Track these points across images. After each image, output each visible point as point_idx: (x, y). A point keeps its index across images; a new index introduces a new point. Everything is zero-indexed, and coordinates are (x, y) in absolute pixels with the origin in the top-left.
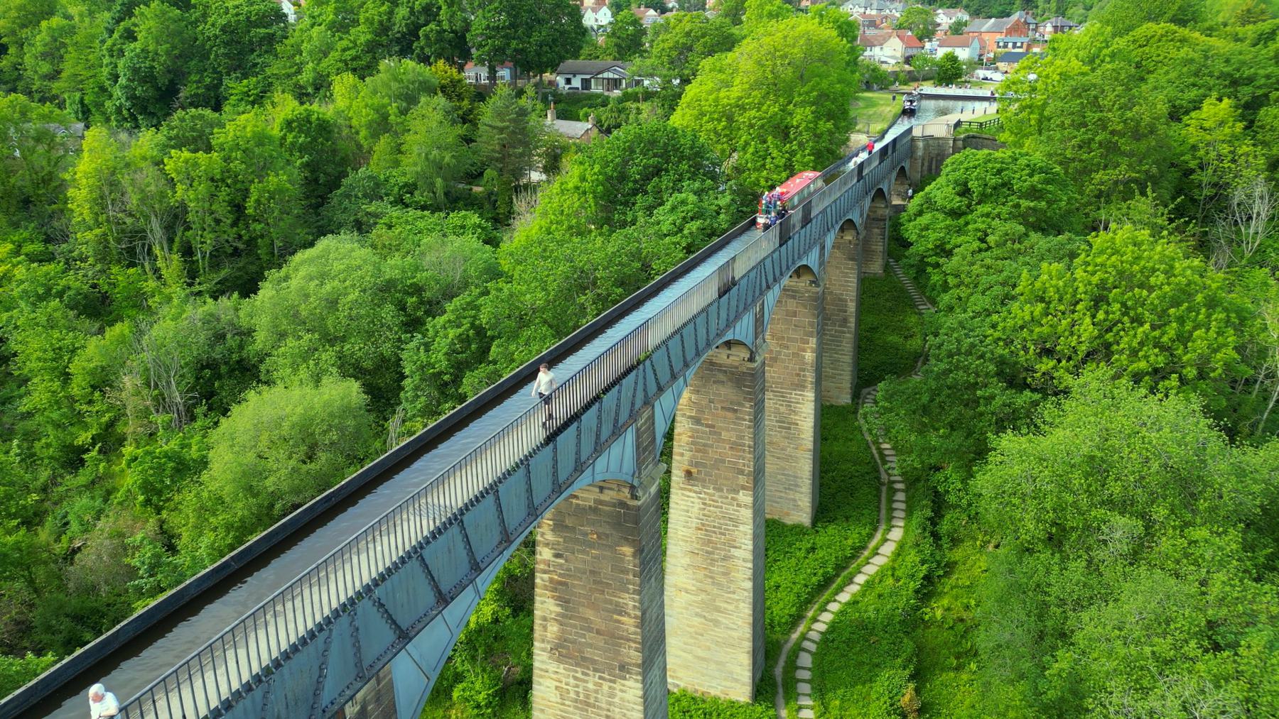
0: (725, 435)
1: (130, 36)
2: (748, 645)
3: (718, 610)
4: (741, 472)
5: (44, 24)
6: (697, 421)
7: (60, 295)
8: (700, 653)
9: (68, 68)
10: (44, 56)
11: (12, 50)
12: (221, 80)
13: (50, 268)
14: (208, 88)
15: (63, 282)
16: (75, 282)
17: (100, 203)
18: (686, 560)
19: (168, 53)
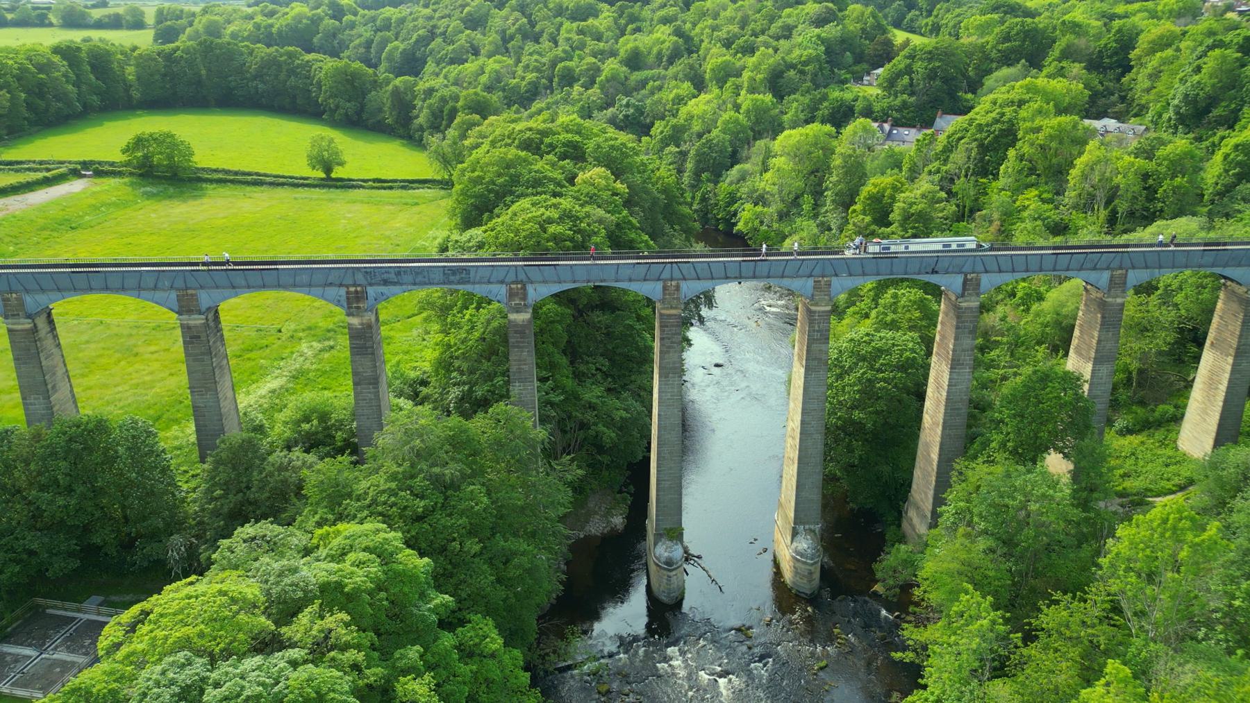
0: (1230, 327)
1: (1198, 70)
2: (1214, 435)
3: (1207, 414)
4: (1231, 347)
5: (1159, 54)
6: (1221, 318)
7: (1043, 220)
8: (1195, 434)
9: (1160, 86)
10: (1150, 76)
11: (1135, 70)
12: (1242, 106)
13: (1046, 206)
14: (1232, 112)
15: (1048, 214)
16: (1054, 216)
17: (1085, 177)
18: (1201, 386)
19: (1213, 85)
